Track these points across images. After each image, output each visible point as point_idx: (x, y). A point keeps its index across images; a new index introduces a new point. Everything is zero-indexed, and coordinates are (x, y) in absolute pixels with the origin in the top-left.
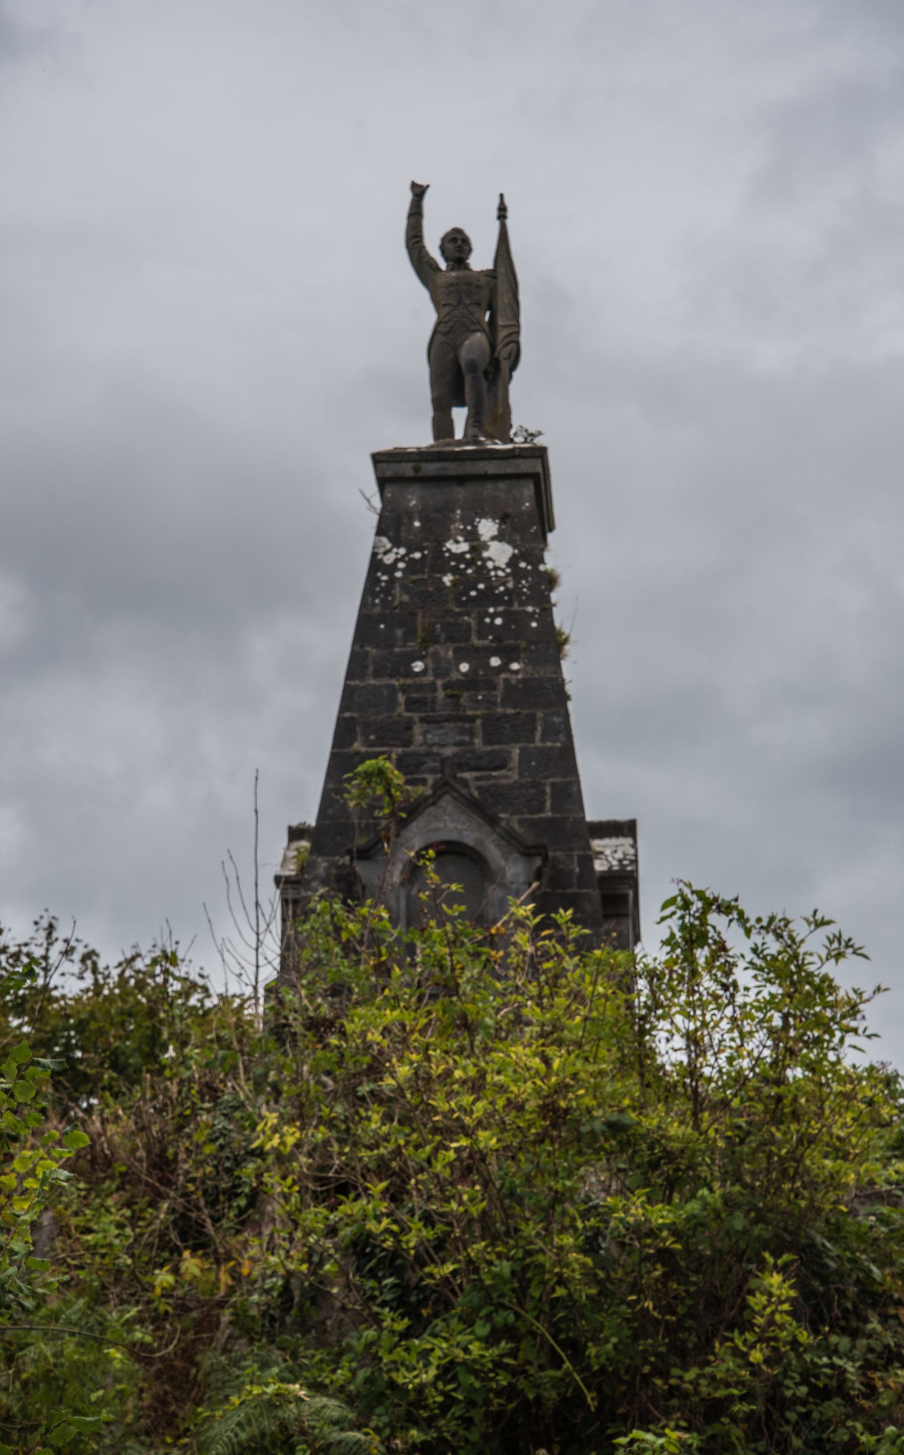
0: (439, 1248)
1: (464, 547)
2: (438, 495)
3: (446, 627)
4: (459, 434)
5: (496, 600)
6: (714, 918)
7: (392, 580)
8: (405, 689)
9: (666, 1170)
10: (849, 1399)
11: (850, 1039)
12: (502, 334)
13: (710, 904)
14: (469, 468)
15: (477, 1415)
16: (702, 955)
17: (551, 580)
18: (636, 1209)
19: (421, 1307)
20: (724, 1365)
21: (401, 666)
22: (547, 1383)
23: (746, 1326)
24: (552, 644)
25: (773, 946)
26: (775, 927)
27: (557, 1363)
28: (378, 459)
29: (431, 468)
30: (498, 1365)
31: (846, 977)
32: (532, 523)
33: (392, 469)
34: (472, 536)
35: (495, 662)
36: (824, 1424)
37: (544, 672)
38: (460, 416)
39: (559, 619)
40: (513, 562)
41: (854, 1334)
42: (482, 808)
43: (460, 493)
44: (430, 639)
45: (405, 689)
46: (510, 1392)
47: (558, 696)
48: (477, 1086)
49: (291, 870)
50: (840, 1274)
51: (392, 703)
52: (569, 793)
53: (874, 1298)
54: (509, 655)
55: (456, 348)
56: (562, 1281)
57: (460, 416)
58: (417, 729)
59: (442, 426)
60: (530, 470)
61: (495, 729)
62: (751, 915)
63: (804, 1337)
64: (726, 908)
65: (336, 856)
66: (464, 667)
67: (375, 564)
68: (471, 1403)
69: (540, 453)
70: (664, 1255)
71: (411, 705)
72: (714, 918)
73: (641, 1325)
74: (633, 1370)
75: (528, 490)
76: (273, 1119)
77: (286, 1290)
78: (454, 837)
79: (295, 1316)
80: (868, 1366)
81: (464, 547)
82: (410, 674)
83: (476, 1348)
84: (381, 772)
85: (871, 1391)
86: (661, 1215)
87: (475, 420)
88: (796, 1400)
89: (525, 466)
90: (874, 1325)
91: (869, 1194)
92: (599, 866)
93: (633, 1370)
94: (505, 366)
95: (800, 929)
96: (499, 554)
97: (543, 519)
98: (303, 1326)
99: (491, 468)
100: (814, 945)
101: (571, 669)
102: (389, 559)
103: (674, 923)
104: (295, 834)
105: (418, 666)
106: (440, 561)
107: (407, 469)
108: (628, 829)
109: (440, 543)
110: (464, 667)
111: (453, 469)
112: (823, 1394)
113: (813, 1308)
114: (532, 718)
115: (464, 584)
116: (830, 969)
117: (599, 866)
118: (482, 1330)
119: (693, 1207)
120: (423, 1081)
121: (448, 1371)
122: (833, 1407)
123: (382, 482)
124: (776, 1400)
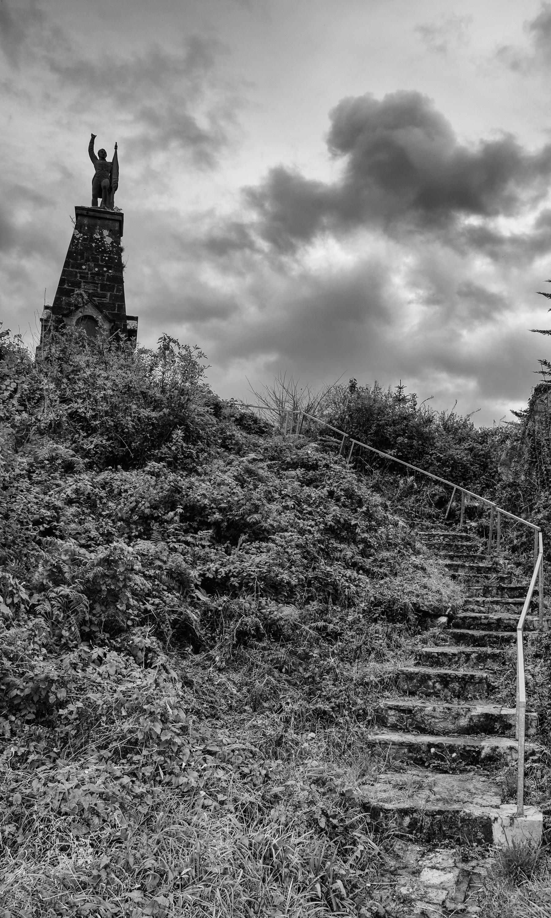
0: (94, 417)
1: (99, 237)
2: (93, 221)
3: (92, 257)
4: (99, 206)
5: (107, 253)
6: (171, 344)
7: (78, 242)
8: (80, 273)
9: (156, 405)
10: (193, 459)
11: (200, 377)
12: (113, 180)
13: (170, 340)
14: (102, 215)
15: (103, 457)
16: (167, 352)
17: (122, 250)
18: (145, 412)
19: (90, 431)
20: (164, 450)
21: (79, 266)
22: (120, 451)
23: (171, 442)
24: (120, 267)
25: (184, 352)
26: (186, 348)
27: (125, 447)
28: (77, 208)
29: (91, 213)
30: (110, 446)
31: (201, 362)
32: (118, 233)
33: (80, 212)
34: (101, 234)
35: (105, 269)
36: (185, 464)
37: (118, 274)
38: (100, 200)
39: (123, 260)
40: (112, 243)
41: (194, 445)
42: (99, 308)
43: (99, 222)
44: (88, 260)
45: (80, 273)
46: (111, 452)
47: (121, 281)
48: (107, 378)
49: (45, 317)
50: (193, 432)
51: (76, 276)
52: (122, 307)
53: (200, 437)
54: (109, 268)
55: (100, 182)
56: (127, 428)
57: (100, 200)
58: (82, 284)
59: (95, 202)
60: (119, 218)
61: (103, 287)
62: (181, 344)
63: (184, 445)
64: (175, 342)
65: (59, 314)
66: (96, 269)
67: (74, 237)
68: (101, 454)
69: (122, 215)
70: (153, 424)
71: (81, 277)
72: (171, 344)
73: (146, 439)
74: (142, 450)
75: (117, 224)
76: (46, 381)
77: (51, 424)
78: (91, 314)
79: (54, 430)
80: (197, 452)
81: (99, 237)
82: (81, 269)
83: (104, 442)
84: (81, 294)
85: (198, 457)
86: (154, 414)
87: (104, 202)
88: (180, 459)
89: (117, 217)
90: (200, 443)
91: (199, 415)
92: (128, 327)
93: (142, 450)
94: (114, 189)
95: (192, 349)
96: (108, 240)
97: (120, 233)
98: (54, 432)
99: (108, 216)
100: (195, 353)
101: (127, 275)
102: (78, 236)
103: (161, 344)
104: (46, 308)
105: (84, 267)
106: (92, 240)
107: (85, 212)
108: (135, 319)
109: (92, 234)
110: (96, 269)
111: (97, 215)
112: (186, 457)
113: (186, 439)
114: (114, 286)
115: (98, 247)
116: (198, 360)
117: (128, 327)
118: (106, 437)
119: (161, 413)
120: (93, 376)
121: (96, 446)
122: (189, 461)
123: (77, 215)
124: (175, 458)
